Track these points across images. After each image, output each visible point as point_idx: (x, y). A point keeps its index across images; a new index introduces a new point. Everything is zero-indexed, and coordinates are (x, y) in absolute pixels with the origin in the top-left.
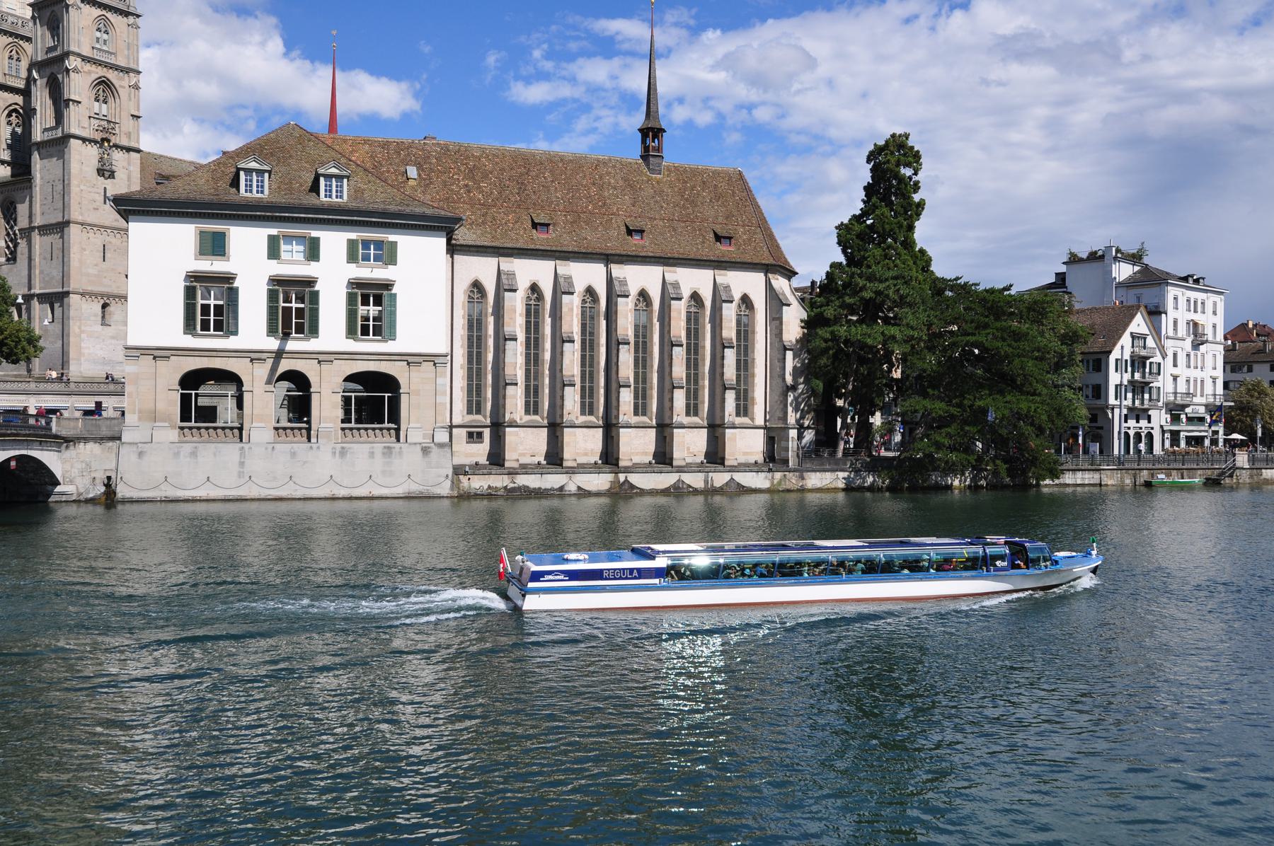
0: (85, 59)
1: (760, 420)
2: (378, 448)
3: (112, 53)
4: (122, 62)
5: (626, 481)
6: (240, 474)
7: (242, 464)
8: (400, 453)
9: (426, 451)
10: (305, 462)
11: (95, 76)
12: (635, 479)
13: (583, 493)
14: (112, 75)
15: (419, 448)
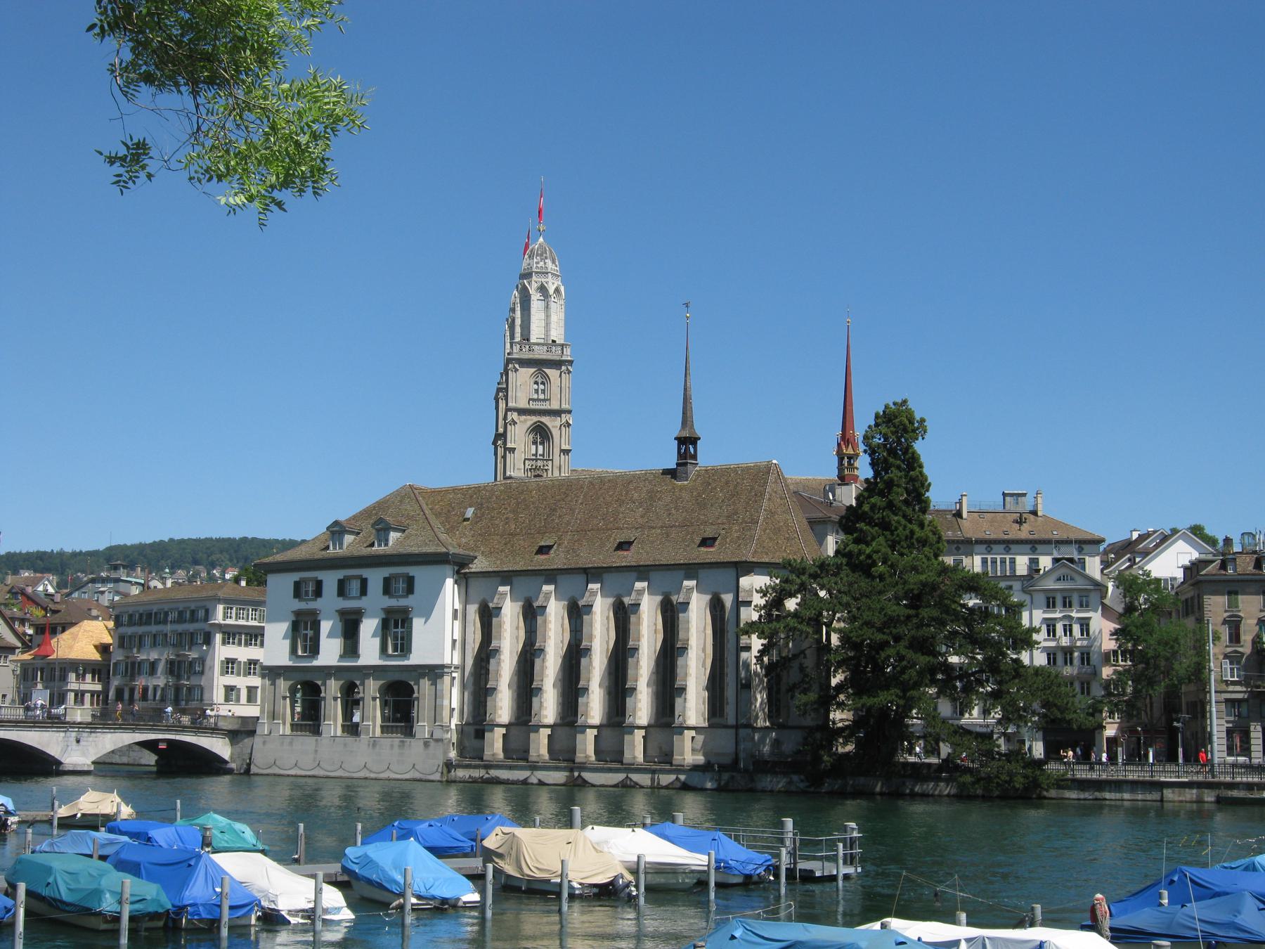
0: (522, 412)
1: (731, 720)
2: (397, 741)
3: (547, 400)
4: (555, 405)
5: (579, 776)
6: (314, 760)
7: (316, 751)
8: (410, 745)
9: (426, 744)
10: (352, 752)
11: (532, 422)
12: (587, 776)
13: (541, 783)
14: (545, 420)
15: (422, 742)
